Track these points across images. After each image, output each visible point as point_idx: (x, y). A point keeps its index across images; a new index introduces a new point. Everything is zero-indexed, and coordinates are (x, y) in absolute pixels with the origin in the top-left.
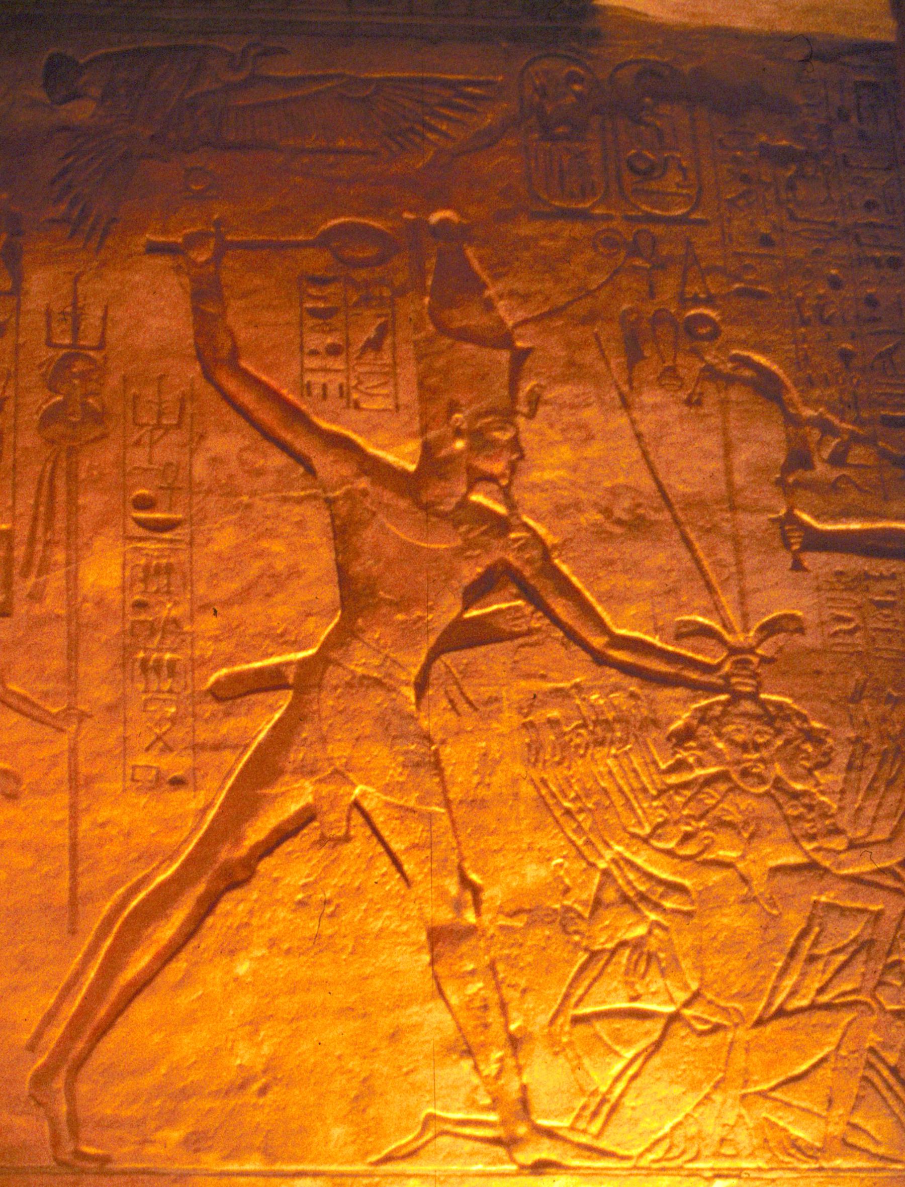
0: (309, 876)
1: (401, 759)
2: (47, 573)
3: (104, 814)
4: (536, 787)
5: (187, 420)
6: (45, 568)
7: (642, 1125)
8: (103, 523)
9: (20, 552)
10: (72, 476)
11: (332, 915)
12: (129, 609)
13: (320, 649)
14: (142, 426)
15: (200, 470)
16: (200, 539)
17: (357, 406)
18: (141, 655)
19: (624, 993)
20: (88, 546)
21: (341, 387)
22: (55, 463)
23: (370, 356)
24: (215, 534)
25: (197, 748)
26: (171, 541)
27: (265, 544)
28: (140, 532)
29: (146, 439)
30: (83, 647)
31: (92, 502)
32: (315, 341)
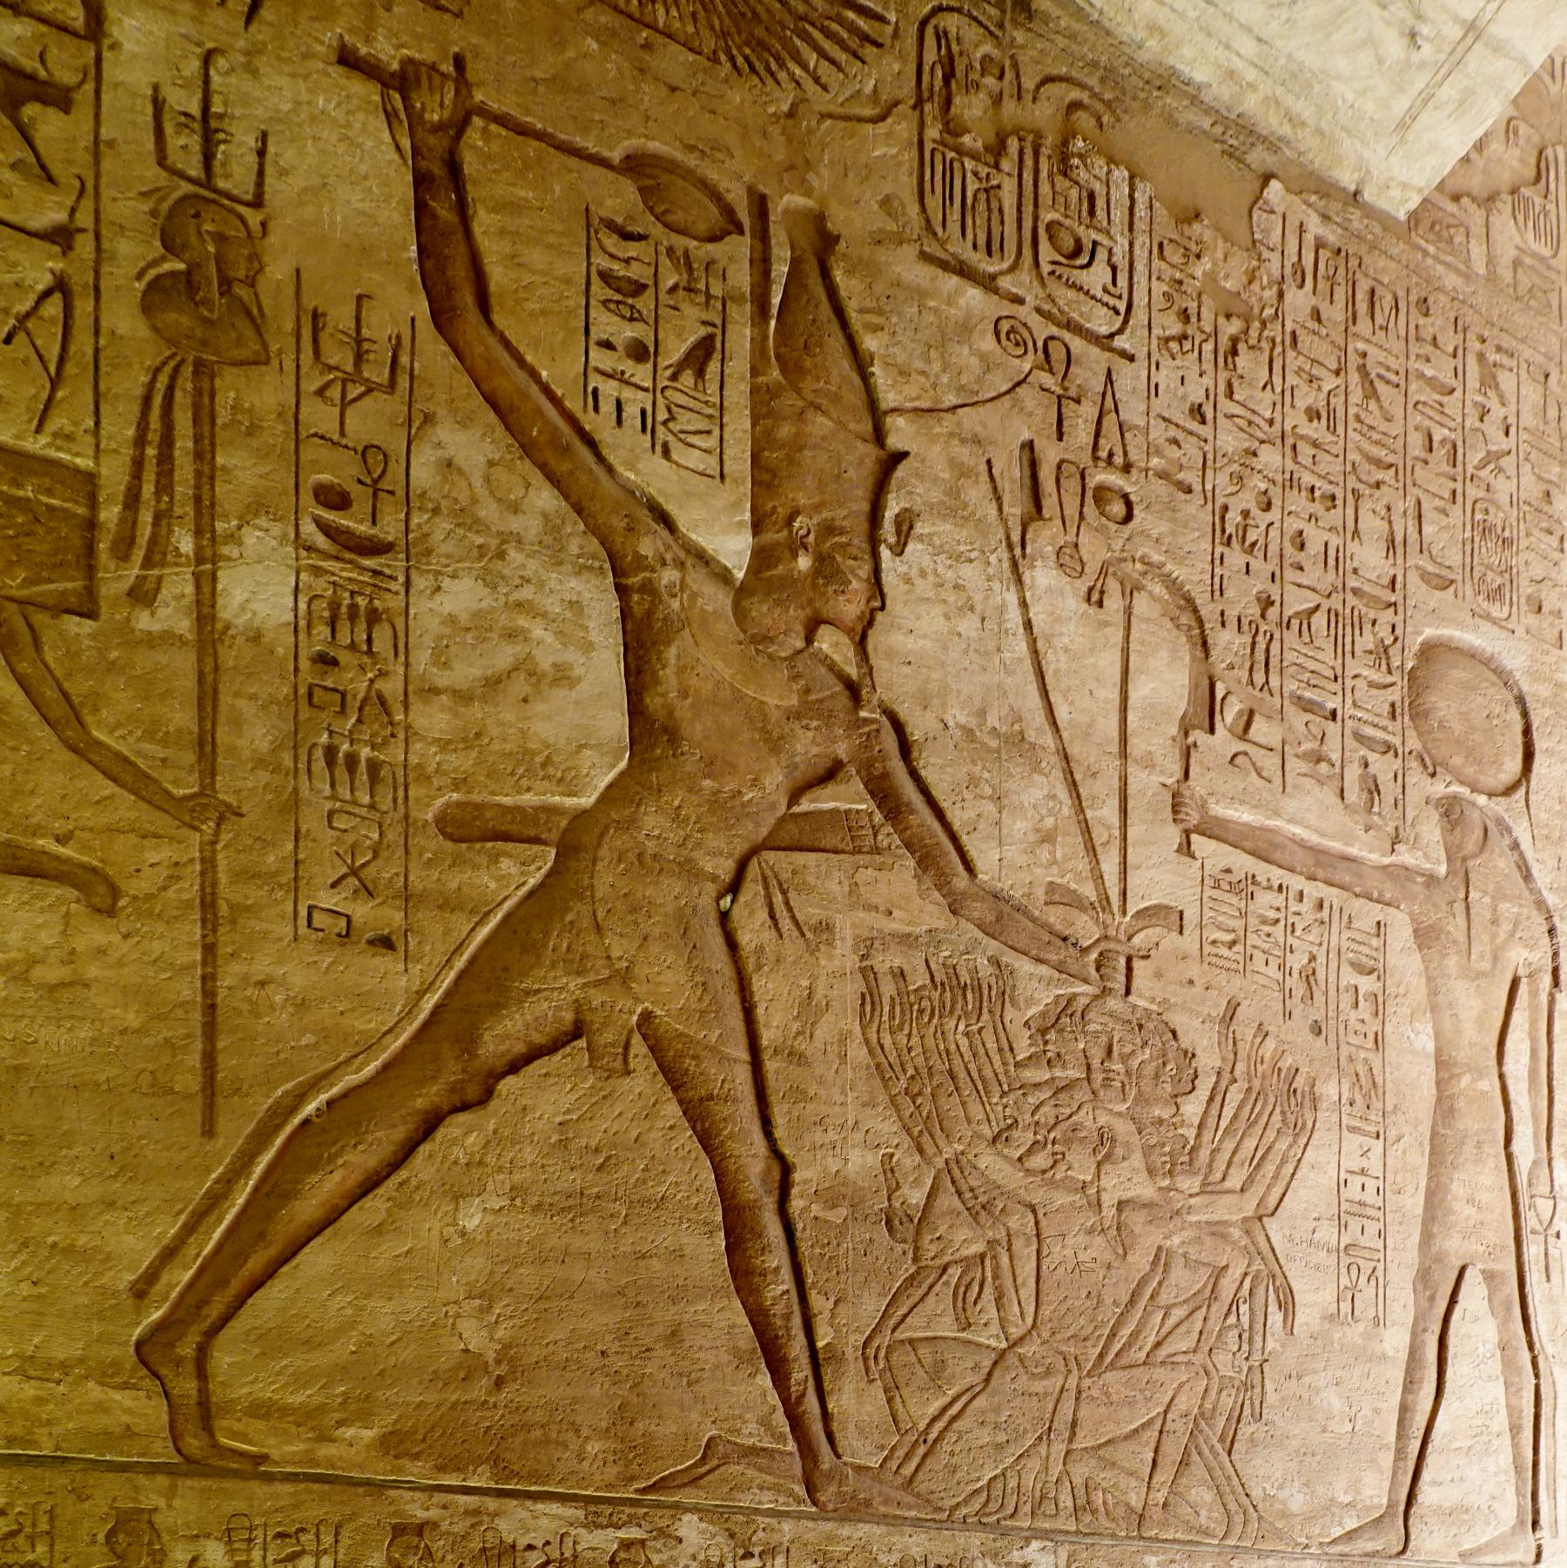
0: (568, 1112)
1: (698, 979)
2: (163, 565)
3: (262, 966)
4: (871, 1052)
5: (403, 382)
6: (157, 554)
7: (959, 1475)
8: (257, 507)
9: (110, 514)
10: (204, 415)
11: (600, 1168)
12: (304, 664)
13: (599, 801)
14: (331, 368)
15: (423, 474)
16: (419, 583)
17: (666, 452)
18: (324, 738)
19: (949, 1319)
20: (233, 538)
21: (643, 412)
22: (173, 377)
23: (687, 378)
24: (446, 583)
25: (408, 898)
26: (376, 573)
27: (523, 622)
28: (321, 541)
29: (335, 392)
30: (225, 699)
31: (242, 471)
32: (607, 324)
